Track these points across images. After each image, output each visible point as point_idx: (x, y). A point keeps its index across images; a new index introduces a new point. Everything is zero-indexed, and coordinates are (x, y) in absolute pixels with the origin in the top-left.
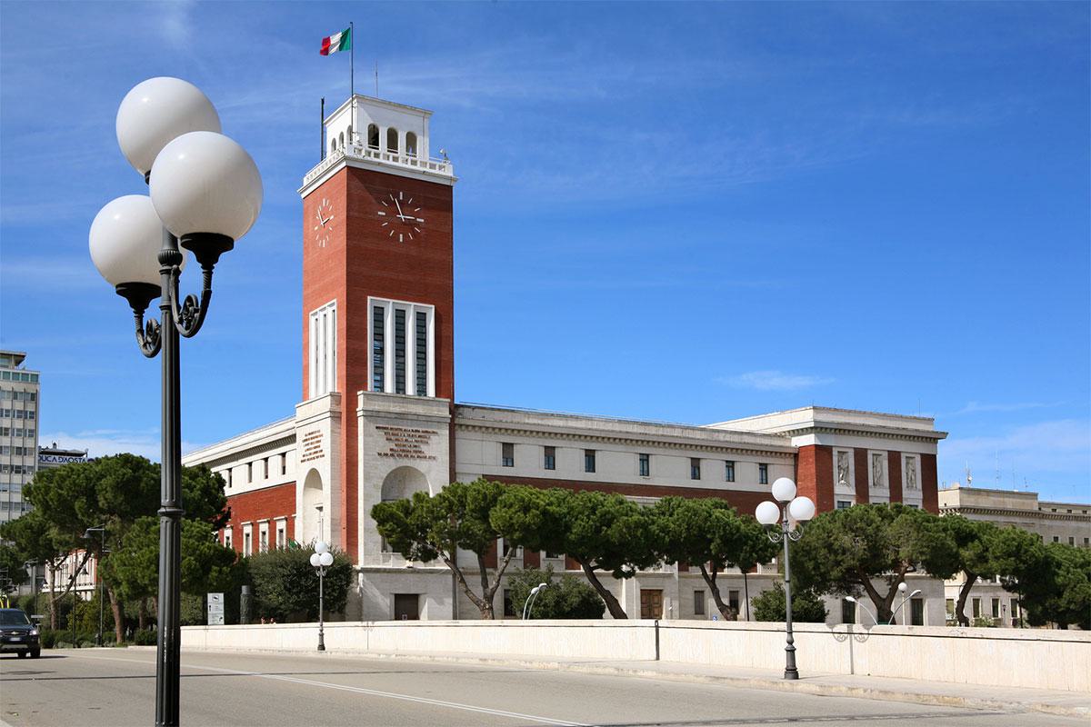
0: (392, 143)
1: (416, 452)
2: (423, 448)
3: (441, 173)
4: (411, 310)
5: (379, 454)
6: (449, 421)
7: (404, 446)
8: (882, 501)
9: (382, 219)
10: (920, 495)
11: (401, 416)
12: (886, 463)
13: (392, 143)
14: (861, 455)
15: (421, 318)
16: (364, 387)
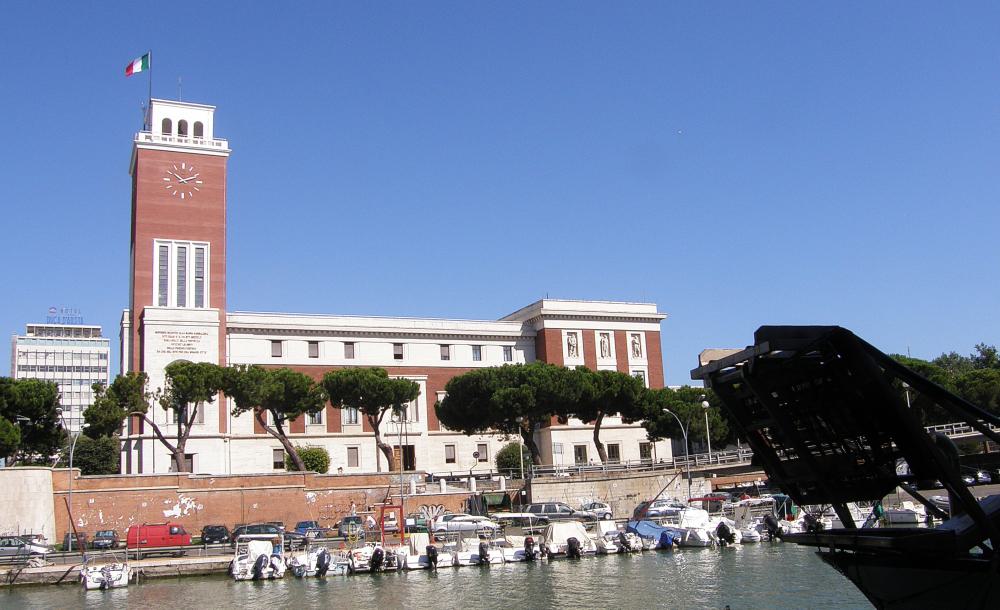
2: (194, 345)
9: (167, 184)
10: (646, 362)
11: (177, 323)
14: (588, 335)
15: (200, 252)
16: (150, 302)
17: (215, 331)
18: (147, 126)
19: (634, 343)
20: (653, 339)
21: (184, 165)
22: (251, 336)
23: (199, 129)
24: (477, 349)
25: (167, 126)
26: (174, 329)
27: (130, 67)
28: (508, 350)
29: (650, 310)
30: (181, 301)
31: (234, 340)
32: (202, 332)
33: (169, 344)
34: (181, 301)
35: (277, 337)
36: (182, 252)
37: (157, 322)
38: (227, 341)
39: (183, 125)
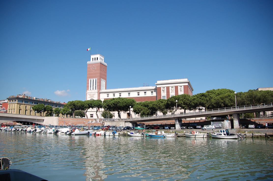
0: (95, 60)
13: (95, 60)
17: (97, 94)
18: (90, 60)
22: (104, 94)
24: (145, 92)
25: (93, 58)
26: (91, 94)
27: (88, 50)
28: (152, 92)
29: (186, 80)
31: (101, 95)
35: (108, 93)
37: (88, 93)
39: (97, 58)
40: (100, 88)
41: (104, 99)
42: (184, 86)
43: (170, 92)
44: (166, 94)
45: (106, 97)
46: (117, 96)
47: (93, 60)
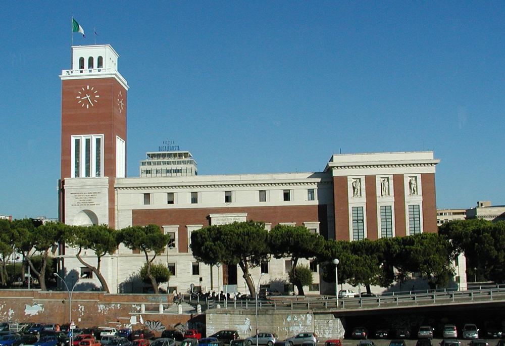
0: (91, 64)
1: (90, 203)
2: (93, 200)
3: (105, 73)
4: (94, 138)
5: (72, 205)
6: (108, 187)
7: (84, 200)
8: (389, 204)
9: (78, 100)
10: (421, 198)
12: (391, 182)
13: (91, 64)
15: (98, 141)
16: (69, 176)
18: (70, 66)
19: (410, 184)
20: (427, 179)
21: (88, 87)
23: (100, 60)
30: (88, 173)
32: (97, 192)
33: (78, 200)
34: (88, 173)
36: (88, 142)
38: (116, 196)
40: (110, 171)
41: (135, 212)
42: (424, 176)
43: (378, 193)
44: (364, 199)
45: (141, 205)
46: (183, 201)
47: (82, 66)
